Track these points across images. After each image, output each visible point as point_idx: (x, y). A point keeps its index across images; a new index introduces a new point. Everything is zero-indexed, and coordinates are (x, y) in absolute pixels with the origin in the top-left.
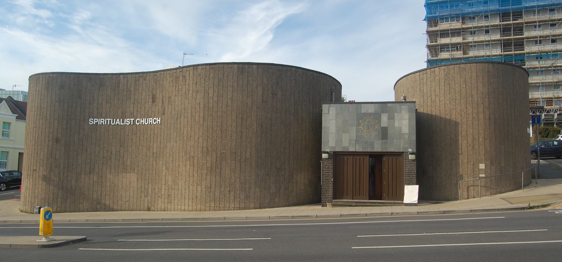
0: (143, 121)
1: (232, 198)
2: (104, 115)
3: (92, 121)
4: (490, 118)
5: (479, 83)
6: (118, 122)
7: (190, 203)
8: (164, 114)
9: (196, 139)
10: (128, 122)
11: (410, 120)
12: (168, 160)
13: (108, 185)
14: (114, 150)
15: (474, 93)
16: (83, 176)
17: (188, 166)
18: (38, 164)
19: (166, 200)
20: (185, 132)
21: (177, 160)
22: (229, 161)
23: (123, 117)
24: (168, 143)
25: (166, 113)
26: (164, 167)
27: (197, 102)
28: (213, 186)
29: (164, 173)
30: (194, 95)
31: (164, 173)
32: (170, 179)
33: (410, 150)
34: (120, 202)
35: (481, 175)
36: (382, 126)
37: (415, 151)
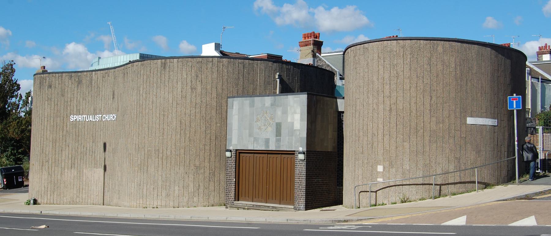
1: (155, 195)
3: (73, 118)
4: (391, 109)
5: (380, 67)
6: (91, 118)
10: (98, 117)
11: (301, 114)
13: (84, 179)
14: (88, 146)
15: (375, 79)
16: (66, 170)
22: (154, 158)
23: (95, 114)
28: (142, 183)
33: (301, 149)
34: (92, 196)
35: (378, 180)
36: (277, 121)
37: (305, 150)
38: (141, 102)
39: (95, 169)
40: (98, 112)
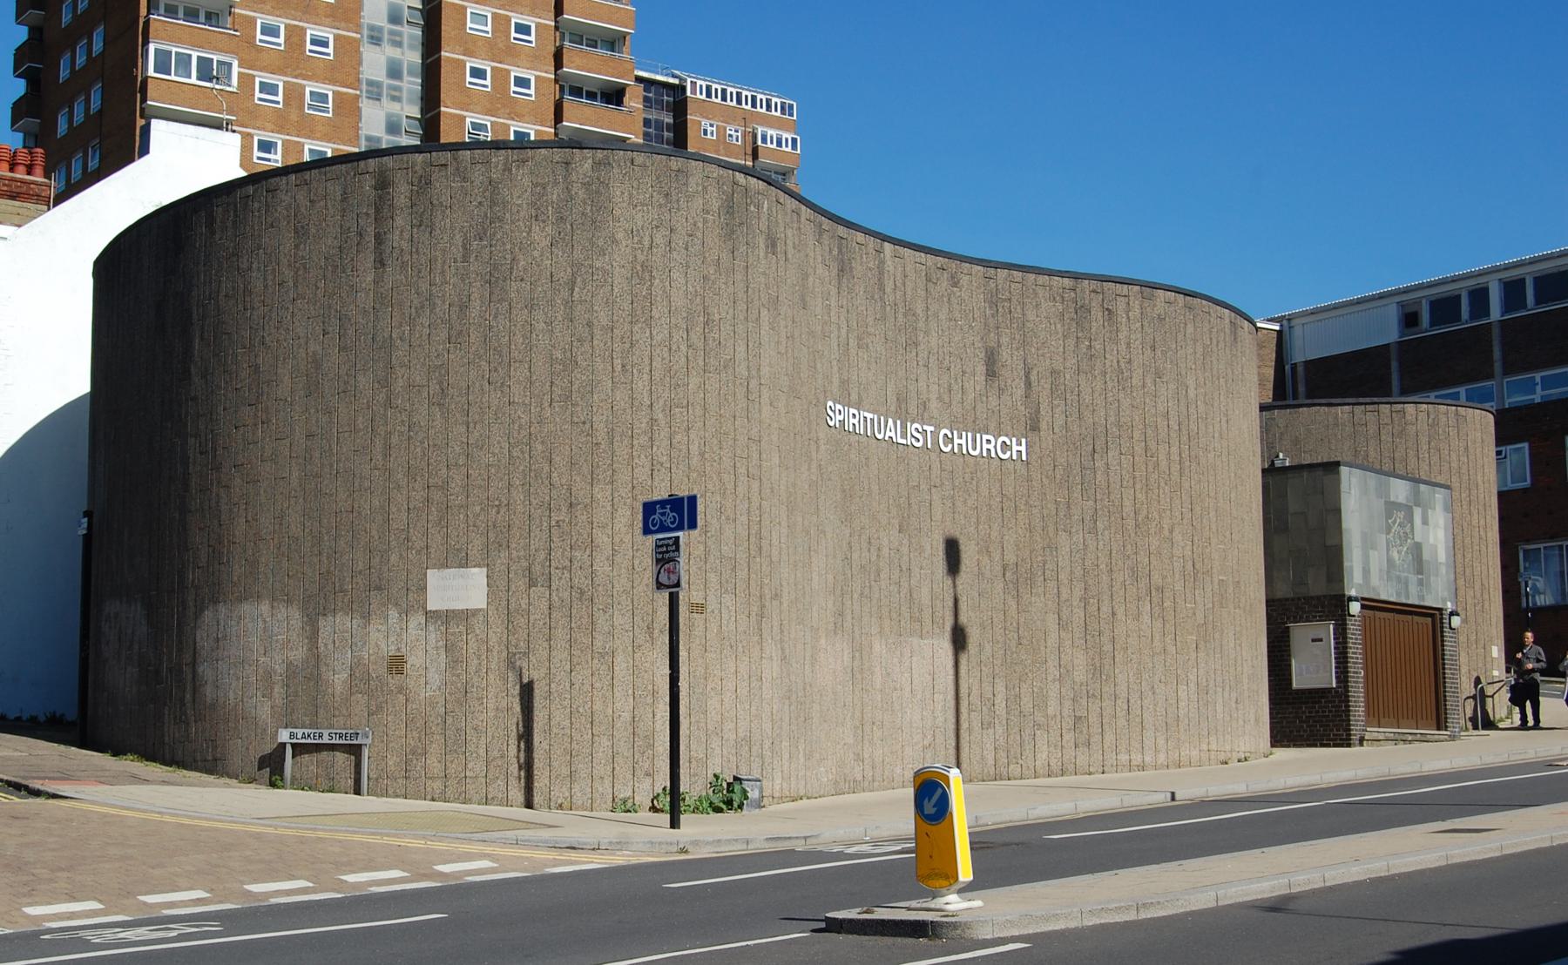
0: (962, 441)
2: (854, 397)
3: (840, 414)
6: (891, 431)
7: (1161, 742)
8: (1034, 427)
9: (1166, 533)
12: (1064, 596)
14: (885, 542)
16: (823, 641)
17: (1146, 618)
18: (713, 577)
19: (1069, 737)
20: (1127, 503)
21: (1106, 597)
24: (1064, 535)
25: (1043, 425)
26: (1052, 620)
27: (1161, 408)
29: (1052, 639)
30: (1149, 381)
31: (1052, 639)
32: (1080, 660)
38: (1193, 427)
39: (915, 641)
40: (913, 410)
